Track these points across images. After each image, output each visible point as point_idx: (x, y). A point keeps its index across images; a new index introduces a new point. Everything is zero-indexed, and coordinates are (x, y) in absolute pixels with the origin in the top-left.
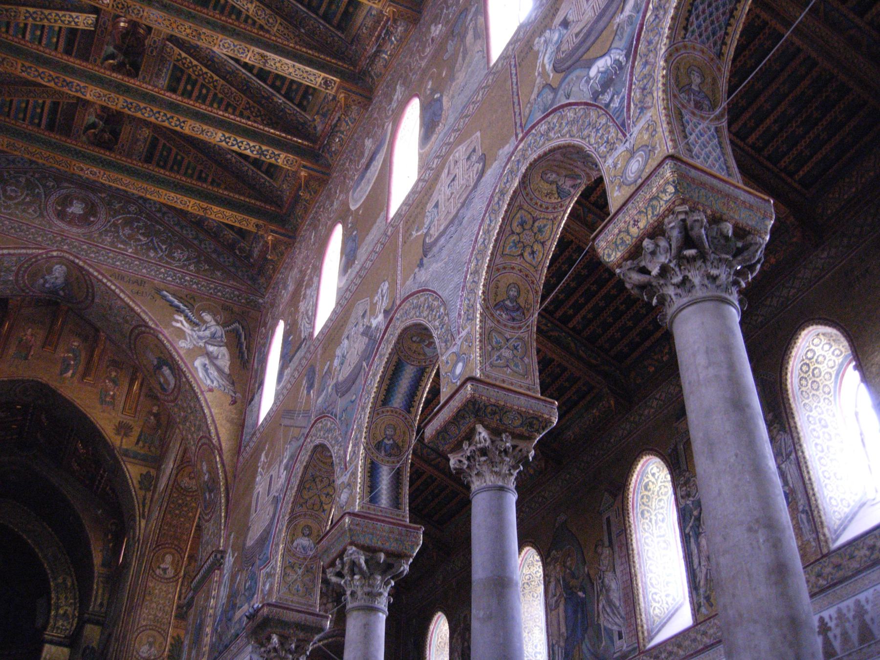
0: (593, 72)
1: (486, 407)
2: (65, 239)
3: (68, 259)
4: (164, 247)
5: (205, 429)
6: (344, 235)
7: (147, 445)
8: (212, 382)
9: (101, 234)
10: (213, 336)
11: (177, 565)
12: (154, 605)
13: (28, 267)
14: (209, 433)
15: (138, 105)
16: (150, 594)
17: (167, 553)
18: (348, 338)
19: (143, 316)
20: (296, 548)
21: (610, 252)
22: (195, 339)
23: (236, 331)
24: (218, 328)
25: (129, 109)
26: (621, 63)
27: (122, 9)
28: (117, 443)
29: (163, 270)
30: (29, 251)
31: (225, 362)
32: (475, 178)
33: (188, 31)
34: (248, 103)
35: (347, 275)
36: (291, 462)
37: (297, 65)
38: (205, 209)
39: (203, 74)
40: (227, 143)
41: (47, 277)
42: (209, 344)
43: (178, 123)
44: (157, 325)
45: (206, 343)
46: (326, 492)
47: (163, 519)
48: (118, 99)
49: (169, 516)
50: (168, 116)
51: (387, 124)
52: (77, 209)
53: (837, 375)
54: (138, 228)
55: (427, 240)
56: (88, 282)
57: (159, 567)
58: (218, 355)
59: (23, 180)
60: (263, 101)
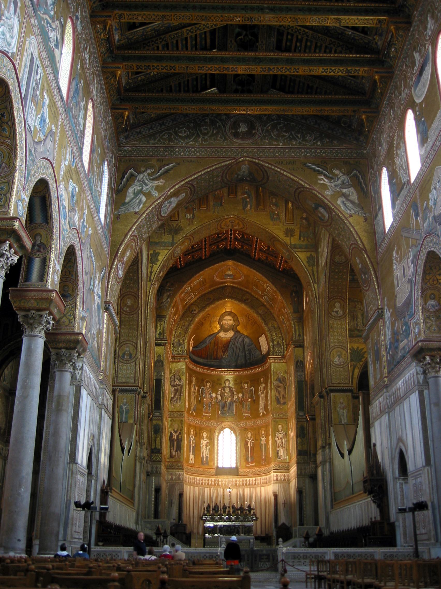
2: (243, 150)
3: (248, 161)
4: (299, 135)
5: (353, 239)
6: (415, 119)
7: (305, 239)
8: (351, 211)
9: (262, 139)
10: (343, 182)
11: (344, 307)
12: (335, 333)
13: (227, 172)
14: (357, 242)
15: (269, 68)
16: (331, 328)
17: (336, 302)
18: (435, 188)
19: (300, 182)
23: (355, 176)
24: (344, 177)
25: (265, 71)
27: (248, 20)
28: (288, 242)
29: (303, 150)
30: (226, 163)
31: (354, 197)
33: (289, 20)
34: (331, 40)
35: (425, 147)
36: (415, 260)
37: (359, 17)
38: (321, 111)
39: (298, 30)
41: (239, 173)
42: (343, 188)
43: (294, 70)
44: (310, 185)
45: (340, 188)
47: (329, 283)
48: (257, 68)
49: (332, 280)
50: (288, 68)
51: (427, 45)
52: (243, 128)
54: (281, 128)
56: (263, 170)
57: (334, 311)
59: (208, 120)
60: (340, 37)
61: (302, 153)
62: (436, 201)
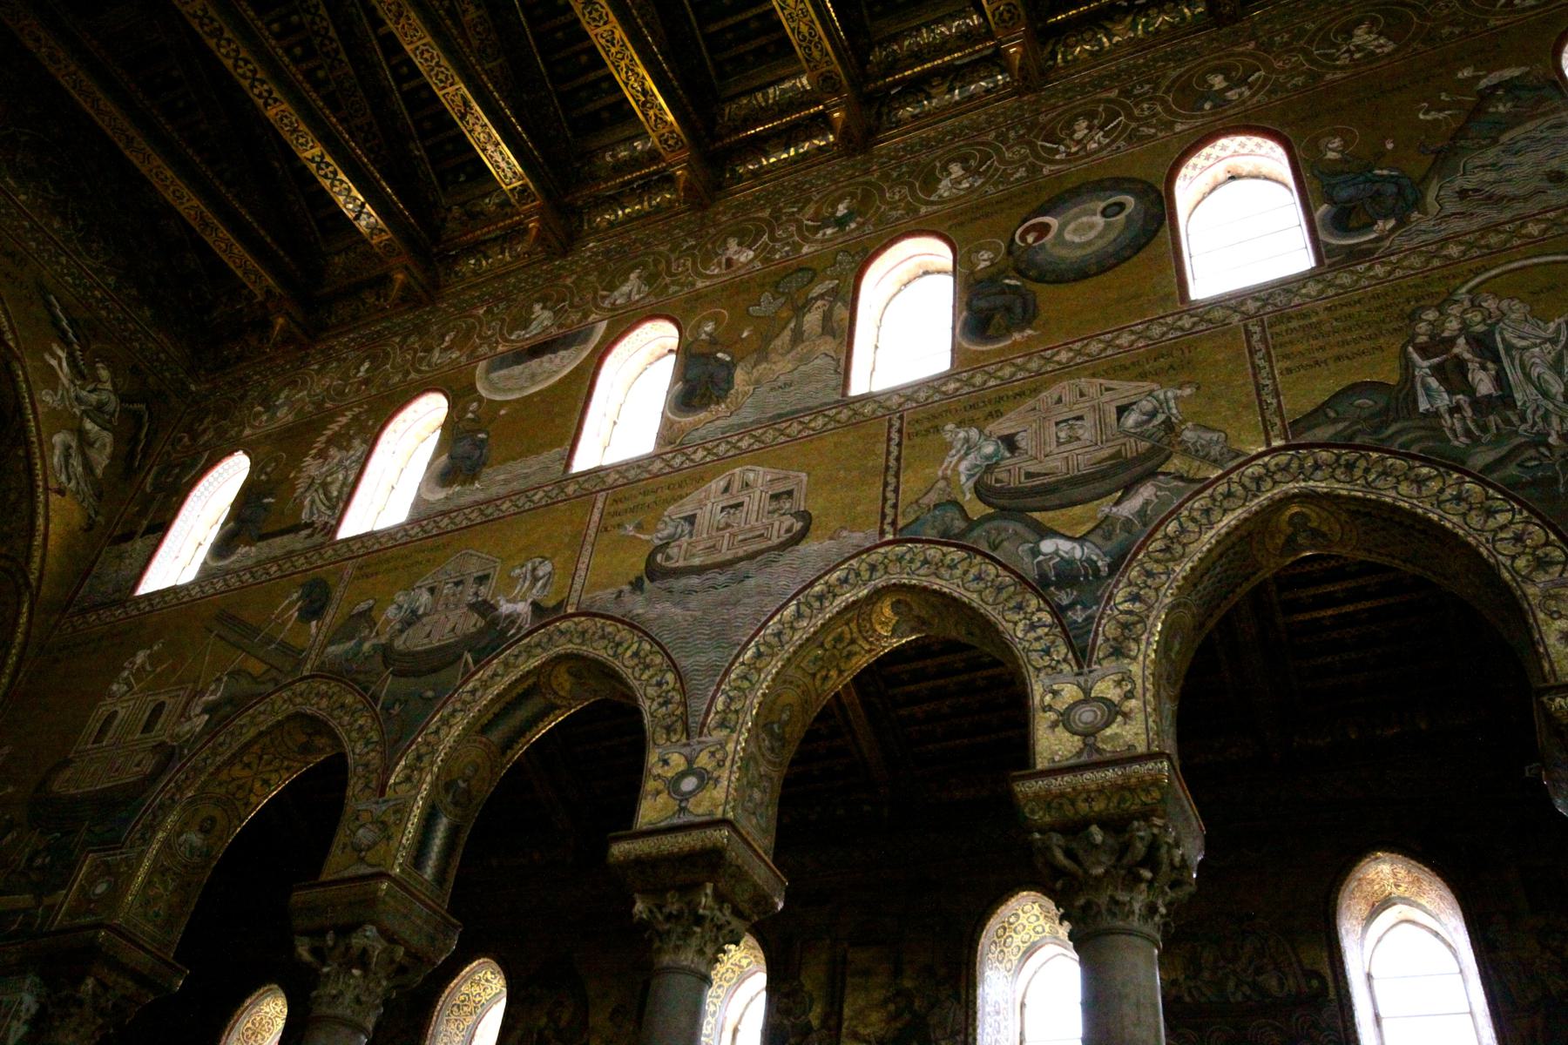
0: (1047, 546)
1: (731, 865)
4: (80, 222)
8: (69, 480)
10: (100, 407)
15: (221, 30)
18: (432, 590)
20: (180, 846)
21: (1036, 809)
22: (69, 398)
24: (113, 397)
25: (202, 25)
26: (1097, 570)
29: (63, 260)
32: (785, 537)
40: (319, 168)
42: (89, 417)
44: (17, 344)
45: (84, 412)
46: (265, 777)
50: (258, 76)
51: (593, 316)
53: (1025, 953)
55: (659, 558)
58: (95, 442)
61: (58, 263)
62: (419, 618)
